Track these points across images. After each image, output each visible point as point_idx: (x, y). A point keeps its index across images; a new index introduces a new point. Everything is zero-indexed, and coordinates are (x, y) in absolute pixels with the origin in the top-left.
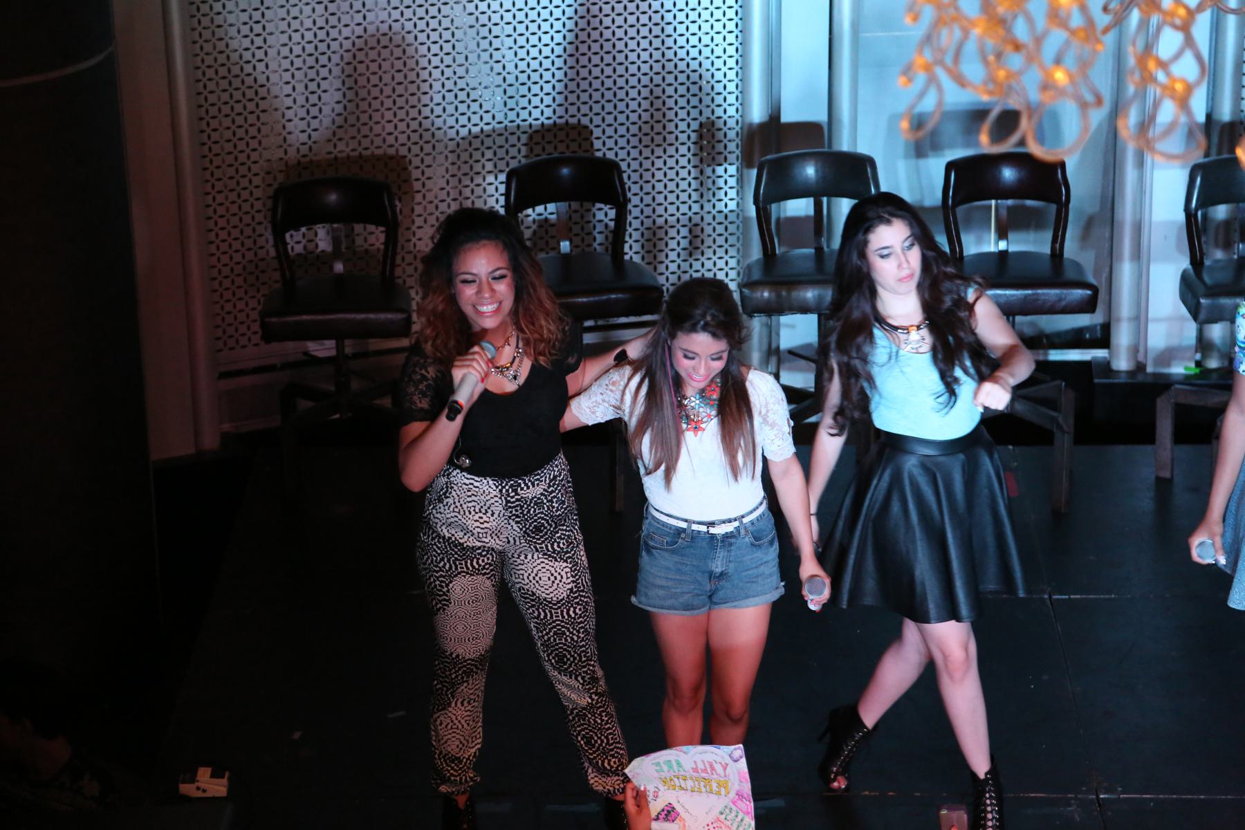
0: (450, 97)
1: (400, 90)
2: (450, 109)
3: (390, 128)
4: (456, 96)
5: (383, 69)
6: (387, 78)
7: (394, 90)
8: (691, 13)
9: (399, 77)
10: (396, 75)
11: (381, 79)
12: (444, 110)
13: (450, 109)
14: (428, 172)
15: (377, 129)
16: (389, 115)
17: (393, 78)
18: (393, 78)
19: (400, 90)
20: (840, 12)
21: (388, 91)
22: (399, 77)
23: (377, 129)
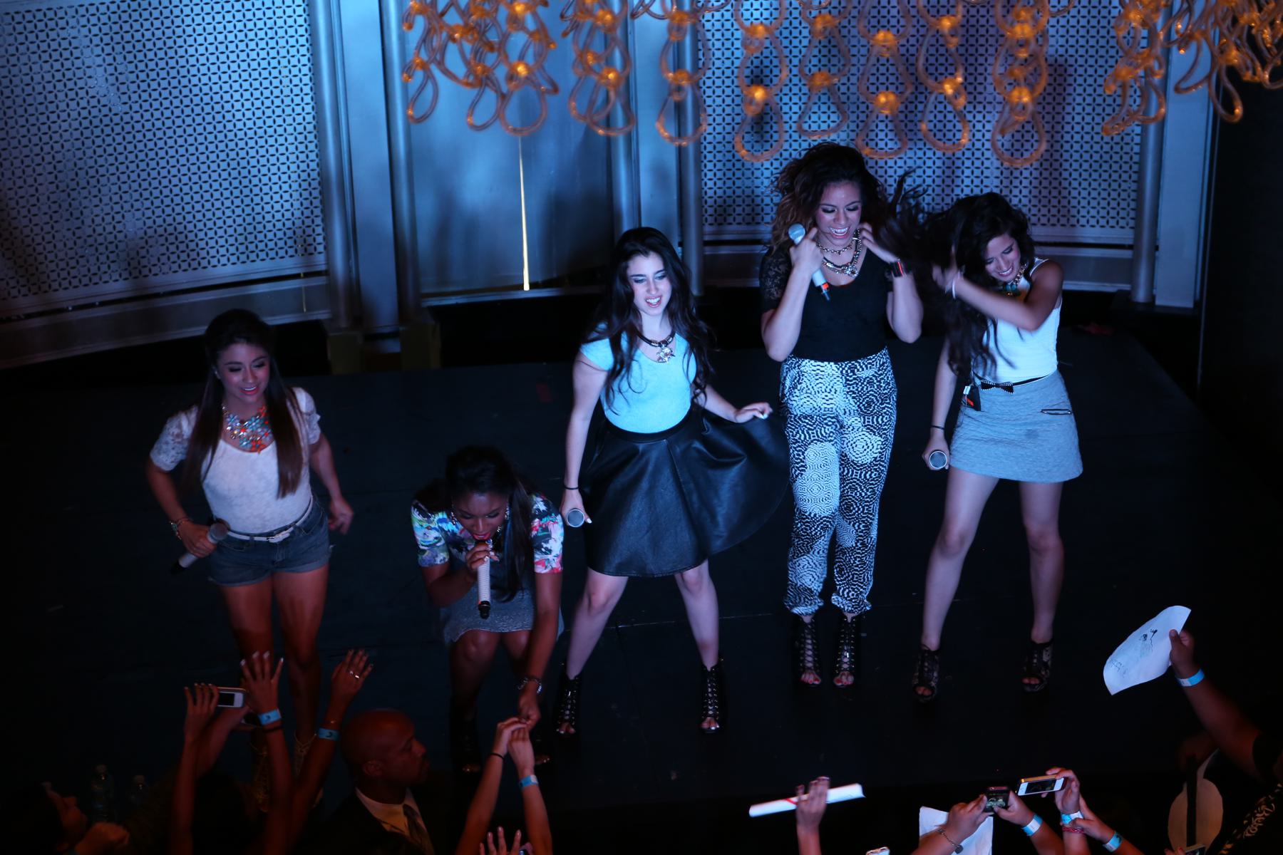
0: (73, 104)
1: (29, 100)
2: (74, 115)
3: (23, 131)
4: (78, 104)
5: (14, 83)
6: (18, 91)
7: (24, 101)
8: (269, 31)
9: (28, 90)
10: (26, 88)
11: (12, 91)
12: (69, 115)
13: (74, 115)
14: (60, 167)
15: (12, 133)
16: (22, 121)
17: (23, 90)
18: (23, 90)
19: (29, 100)
20: (389, 28)
21: (19, 101)
22: (28, 90)
23: (12, 133)
